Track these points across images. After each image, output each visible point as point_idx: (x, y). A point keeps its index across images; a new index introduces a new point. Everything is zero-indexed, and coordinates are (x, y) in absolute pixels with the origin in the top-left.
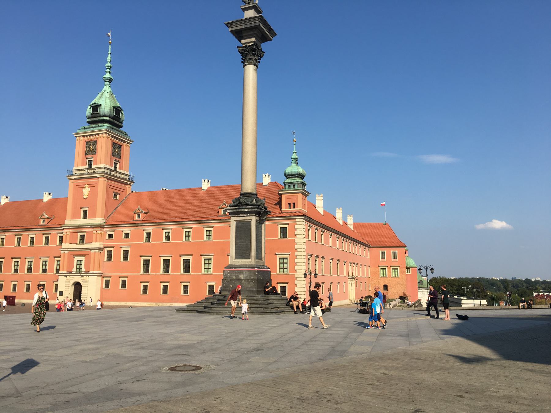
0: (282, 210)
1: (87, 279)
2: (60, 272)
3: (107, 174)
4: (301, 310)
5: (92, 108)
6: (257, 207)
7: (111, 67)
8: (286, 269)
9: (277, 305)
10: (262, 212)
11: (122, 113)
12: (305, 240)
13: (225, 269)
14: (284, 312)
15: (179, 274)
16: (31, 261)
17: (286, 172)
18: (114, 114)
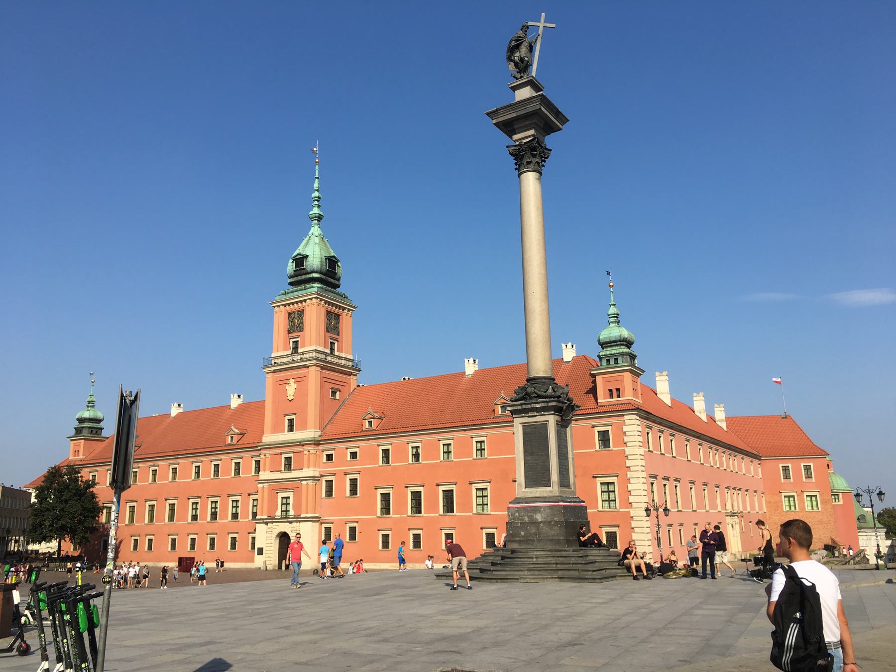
0: (598, 401)
1: (298, 528)
2: (257, 517)
3: (320, 361)
4: (645, 574)
5: (294, 262)
6: (556, 399)
7: (319, 198)
8: (614, 502)
9: (603, 566)
10: (565, 407)
11: (338, 266)
12: (642, 451)
13: (510, 505)
14: (615, 576)
15: (437, 515)
16: (216, 502)
17: (600, 338)
18: (328, 268)
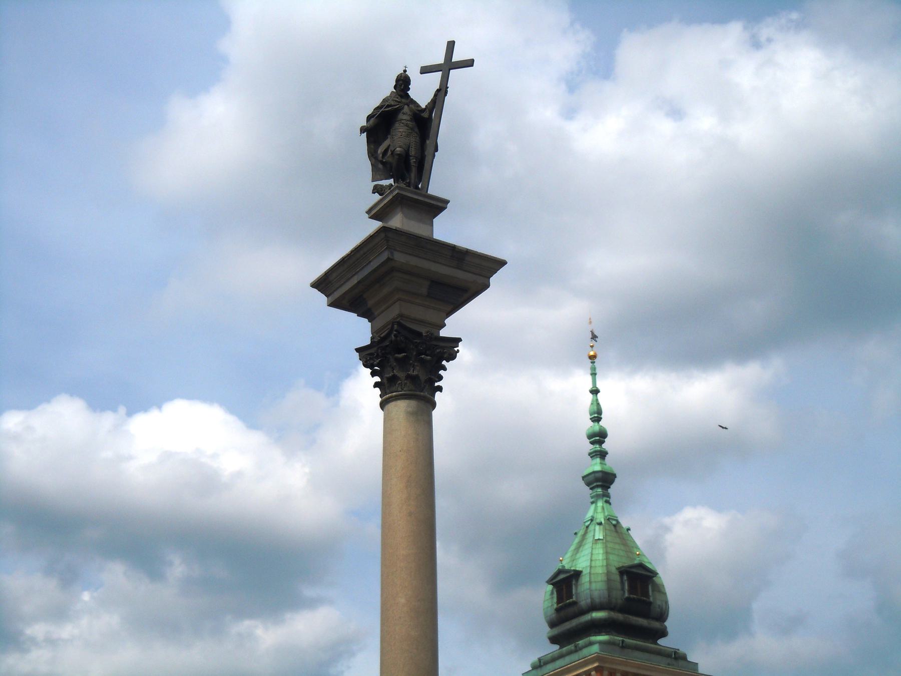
18: (626, 595)
